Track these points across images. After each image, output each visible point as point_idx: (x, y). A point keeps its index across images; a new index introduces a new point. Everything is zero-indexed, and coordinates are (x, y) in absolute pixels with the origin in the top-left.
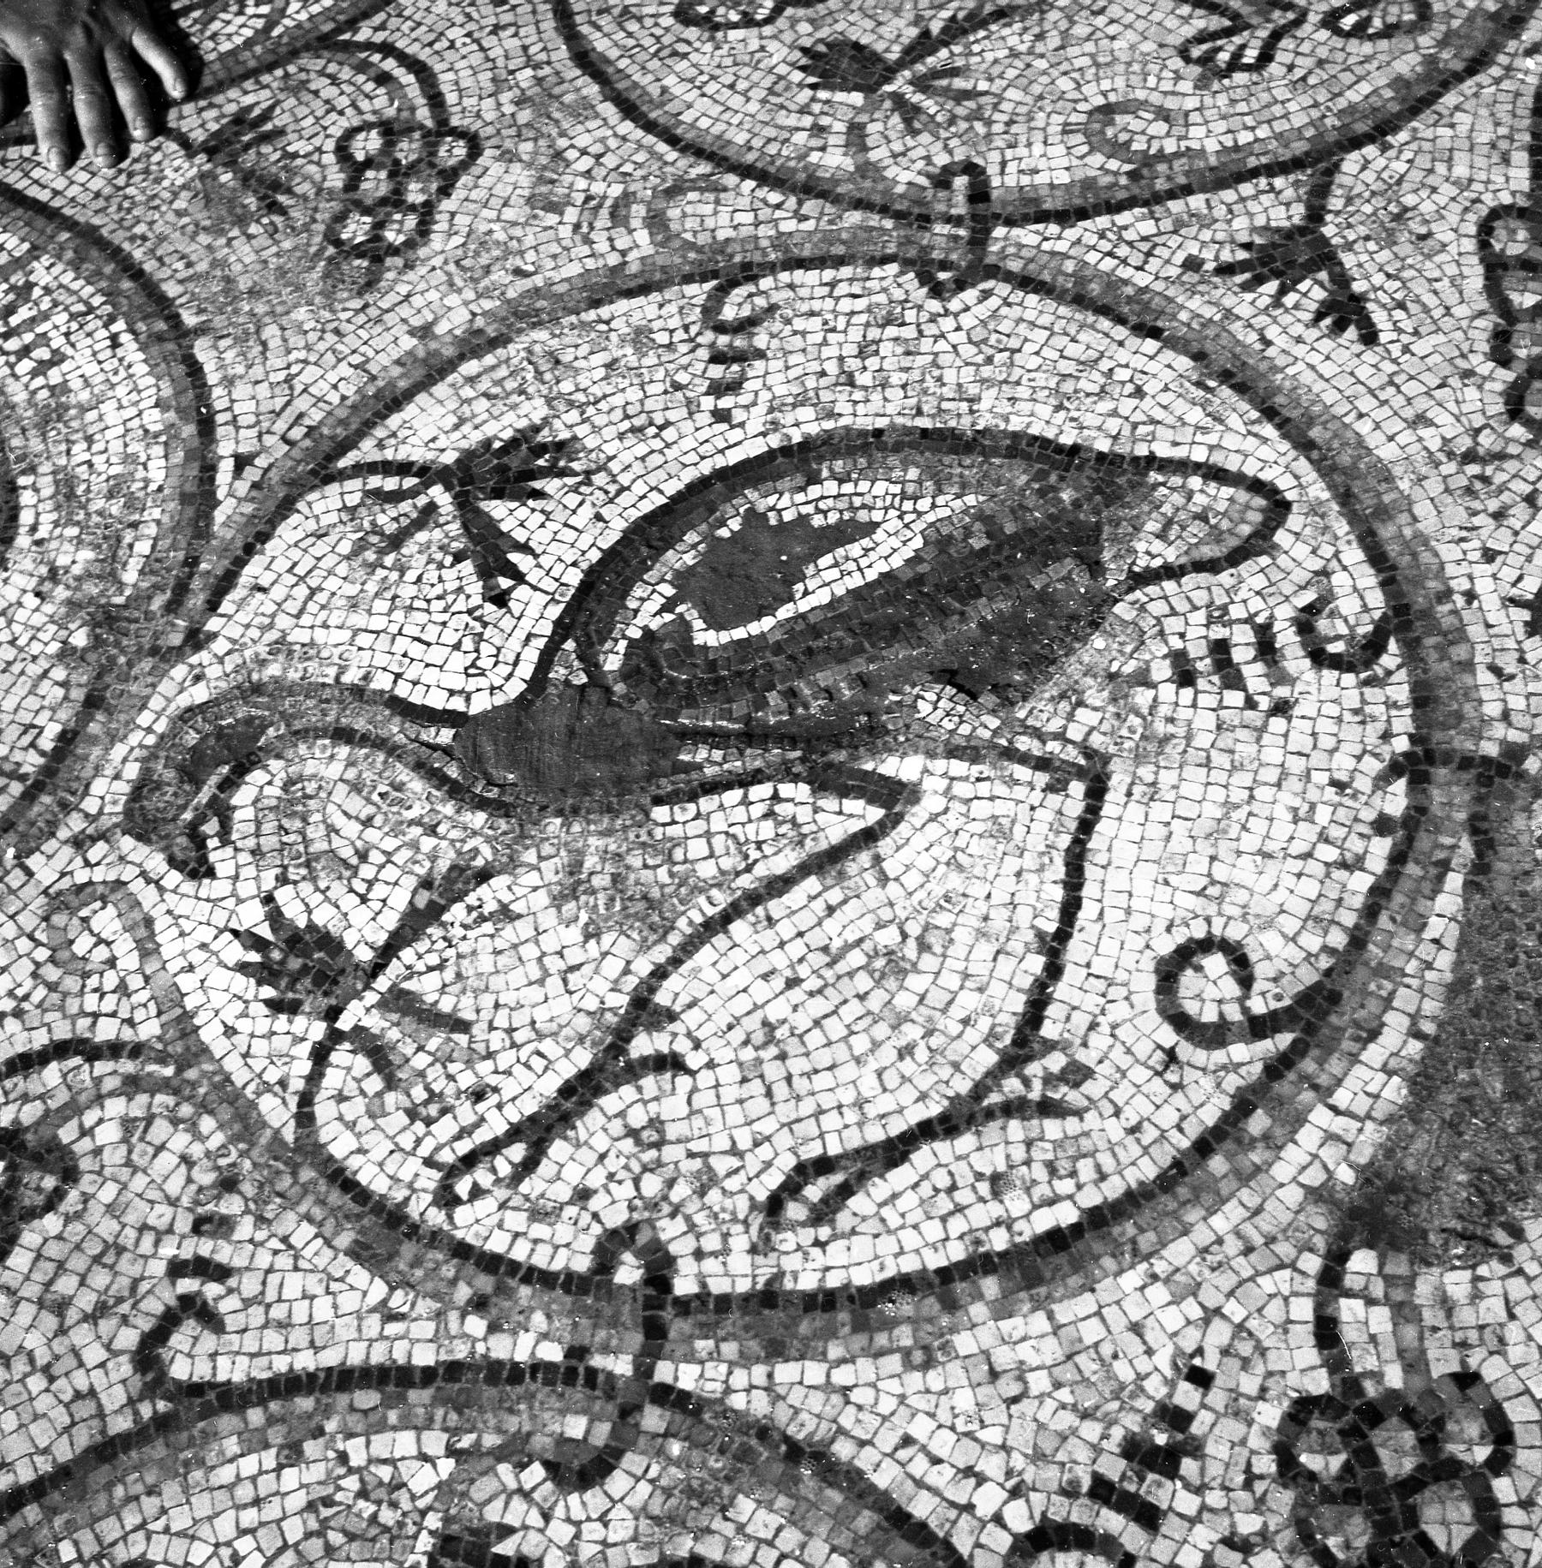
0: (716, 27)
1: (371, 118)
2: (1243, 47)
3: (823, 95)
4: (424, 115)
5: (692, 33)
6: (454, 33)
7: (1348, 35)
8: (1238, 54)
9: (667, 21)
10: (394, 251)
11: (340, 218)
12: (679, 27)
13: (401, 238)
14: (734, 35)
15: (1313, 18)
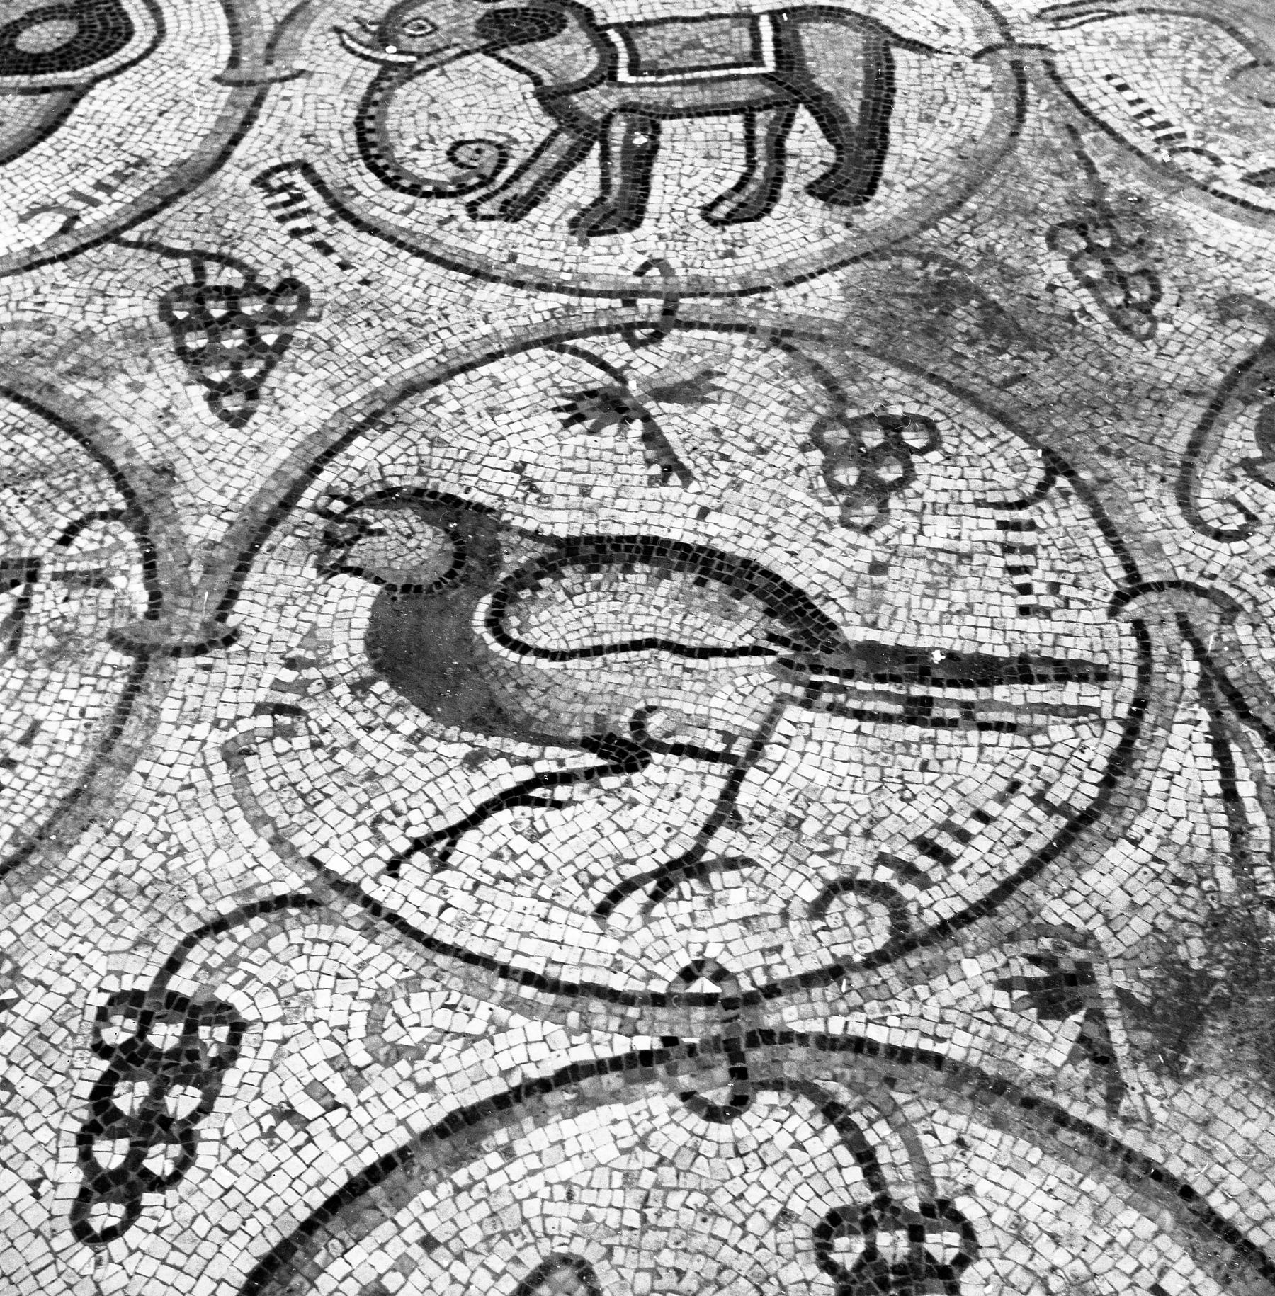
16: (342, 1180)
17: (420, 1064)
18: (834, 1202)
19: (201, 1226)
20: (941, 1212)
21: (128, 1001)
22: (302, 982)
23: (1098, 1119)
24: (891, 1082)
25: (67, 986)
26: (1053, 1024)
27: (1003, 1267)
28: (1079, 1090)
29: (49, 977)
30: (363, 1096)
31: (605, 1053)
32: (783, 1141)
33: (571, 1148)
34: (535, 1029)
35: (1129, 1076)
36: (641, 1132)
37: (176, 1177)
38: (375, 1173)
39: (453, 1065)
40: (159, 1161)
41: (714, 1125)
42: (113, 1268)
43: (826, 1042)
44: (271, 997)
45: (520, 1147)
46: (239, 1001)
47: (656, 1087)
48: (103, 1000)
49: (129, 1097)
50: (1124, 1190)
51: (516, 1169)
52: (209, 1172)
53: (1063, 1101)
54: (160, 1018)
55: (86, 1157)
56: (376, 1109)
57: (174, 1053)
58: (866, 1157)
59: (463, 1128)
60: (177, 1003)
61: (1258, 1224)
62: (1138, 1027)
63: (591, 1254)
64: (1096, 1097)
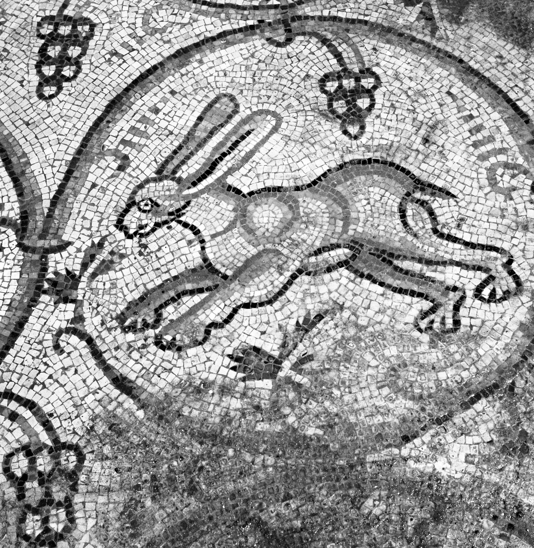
0: (179, 349)
1: (16, 446)
2: (443, 318)
3: (250, 383)
4: (45, 438)
5: (169, 354)
6: (42, 377)
7: (489, 301)
8: (443, 323)
9: (153, 348)
10: (60, 537)
11: (22, 520)
12: (160, 352)
13: (61, 527)
14: (191, 352)
15: (470, 294)
16: (138, 74)
17: (164, 35)
18: (327, 71)
19: (86, 92)
20: (368, 72)
21: (49, 19)
22: (116, 9)
23: (427, 39)
24: (348, 30)
25: (25, 16)
26: (410, 8)
27: (391, 89)
28: (420, 30)
29: (17, 13)
30: (143, 46)
31: (236, 27)
32: (306, 52)
33: (225, 59)
34: (208, 20)
35: (439, 24)
36: (251, 52)
37: (75, 77)
38: (150, 72)
39: (178, 34)
40: (67, 72)
41: (279, 48)
42: (54, 107)
43: (322, 18)
44: (104, 15)
45: (205, 60)
46: (92, 17)
47: (257, 37)
48: (39, 19)
49: (53, 52)
50: (437, 62)
51: (204, 67)
52: (87, 74)
53: (414, 34)
54: (62, 24)
55: (39, 72)
56: (149, 50)
57: (69, 36)
58: (338, 56)
59: (183, 55)
60: (68, 19)
61: (488, 70)
62: (443, 8)
63: (235, 93)
64: (426, 31)
